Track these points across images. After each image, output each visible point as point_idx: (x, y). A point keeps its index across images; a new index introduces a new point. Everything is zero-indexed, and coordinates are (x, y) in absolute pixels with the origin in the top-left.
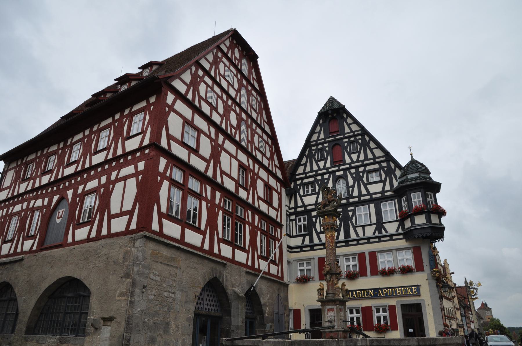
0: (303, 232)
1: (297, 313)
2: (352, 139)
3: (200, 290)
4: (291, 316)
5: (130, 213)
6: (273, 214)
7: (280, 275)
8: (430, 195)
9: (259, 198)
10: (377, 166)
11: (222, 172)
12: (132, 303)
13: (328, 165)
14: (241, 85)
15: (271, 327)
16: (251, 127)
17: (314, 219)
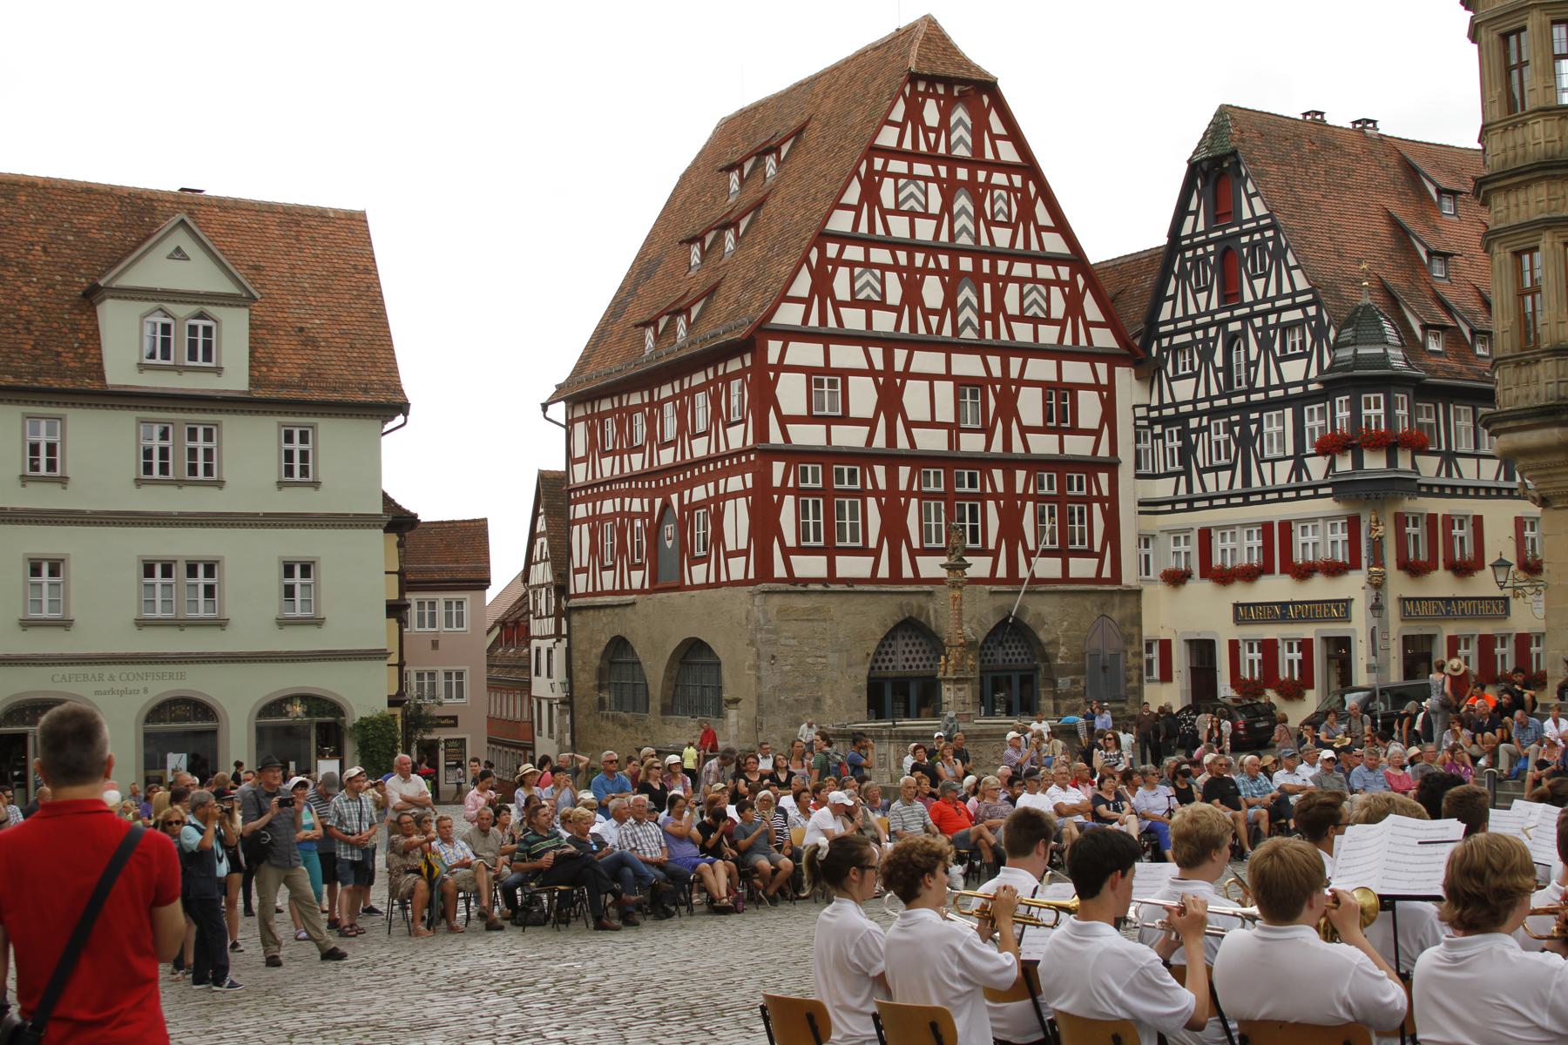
0: (1178, 467)
1: (1166, 646)
2: (1257, 237)
3: (875, 644)
4: (1156, 653)
5: (746, 553)
6: (1078, 446)
7: (1106, 573)
8: (1377, 400)
9: (1024, 430)
10: (1297, 314)
11: (910, 425)
12: (759, 678)
13: (1214, 305)
14: (950, 191)
15: (1073, 682)
16: (993, 277)
17: (1193, 436)
